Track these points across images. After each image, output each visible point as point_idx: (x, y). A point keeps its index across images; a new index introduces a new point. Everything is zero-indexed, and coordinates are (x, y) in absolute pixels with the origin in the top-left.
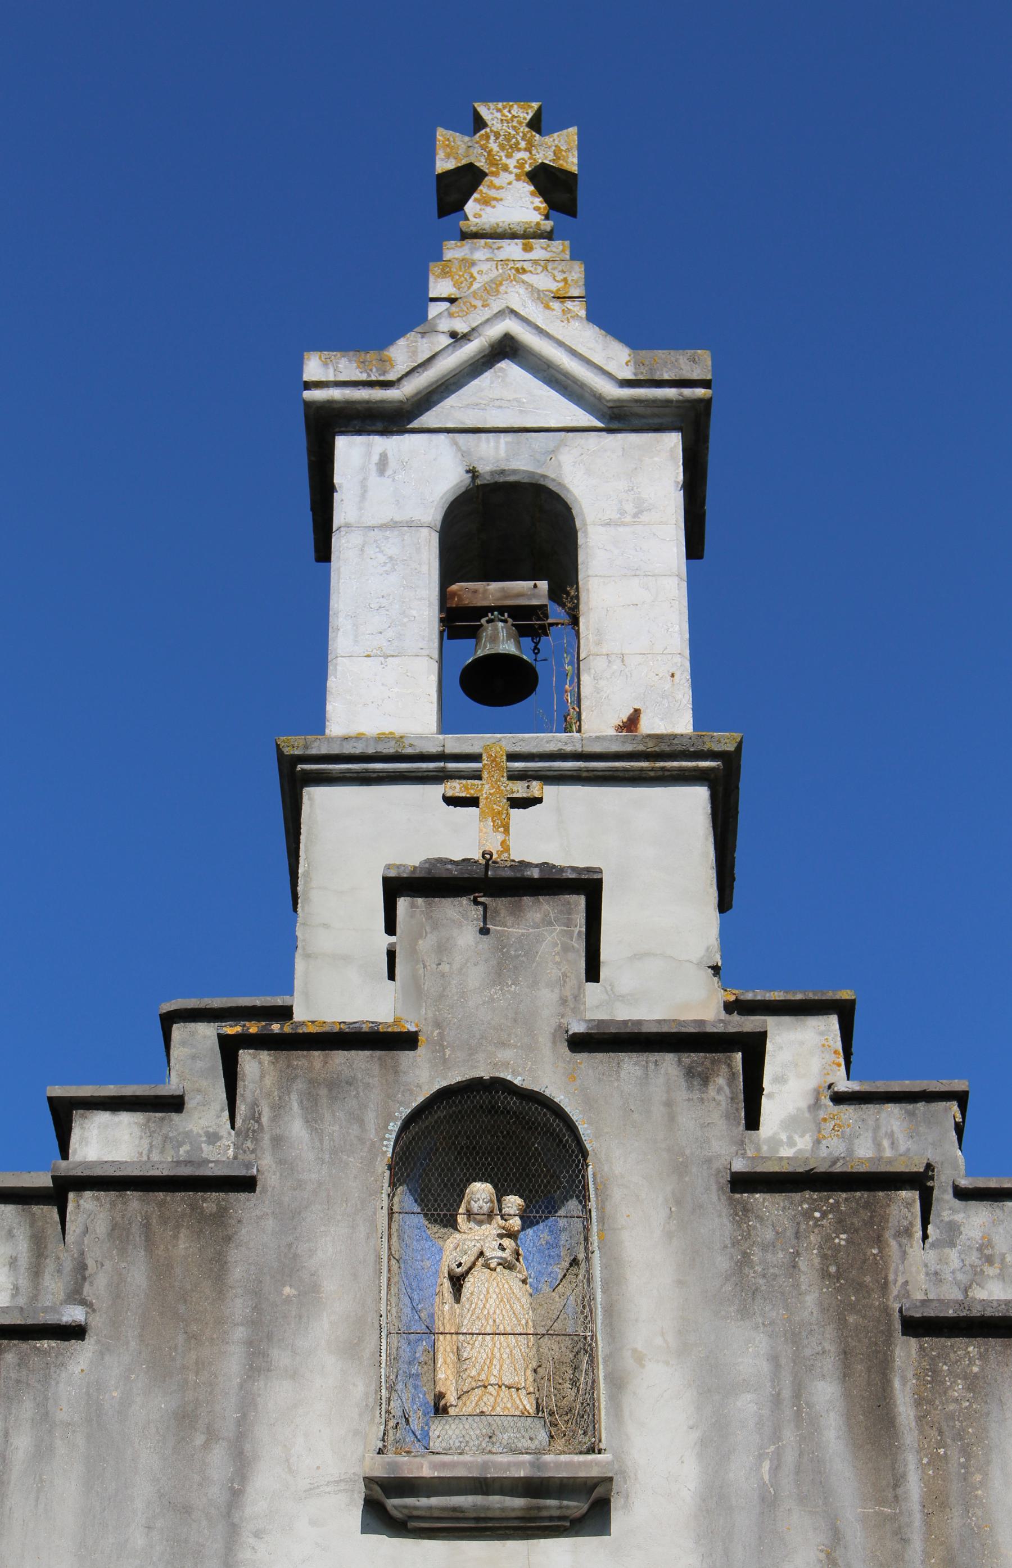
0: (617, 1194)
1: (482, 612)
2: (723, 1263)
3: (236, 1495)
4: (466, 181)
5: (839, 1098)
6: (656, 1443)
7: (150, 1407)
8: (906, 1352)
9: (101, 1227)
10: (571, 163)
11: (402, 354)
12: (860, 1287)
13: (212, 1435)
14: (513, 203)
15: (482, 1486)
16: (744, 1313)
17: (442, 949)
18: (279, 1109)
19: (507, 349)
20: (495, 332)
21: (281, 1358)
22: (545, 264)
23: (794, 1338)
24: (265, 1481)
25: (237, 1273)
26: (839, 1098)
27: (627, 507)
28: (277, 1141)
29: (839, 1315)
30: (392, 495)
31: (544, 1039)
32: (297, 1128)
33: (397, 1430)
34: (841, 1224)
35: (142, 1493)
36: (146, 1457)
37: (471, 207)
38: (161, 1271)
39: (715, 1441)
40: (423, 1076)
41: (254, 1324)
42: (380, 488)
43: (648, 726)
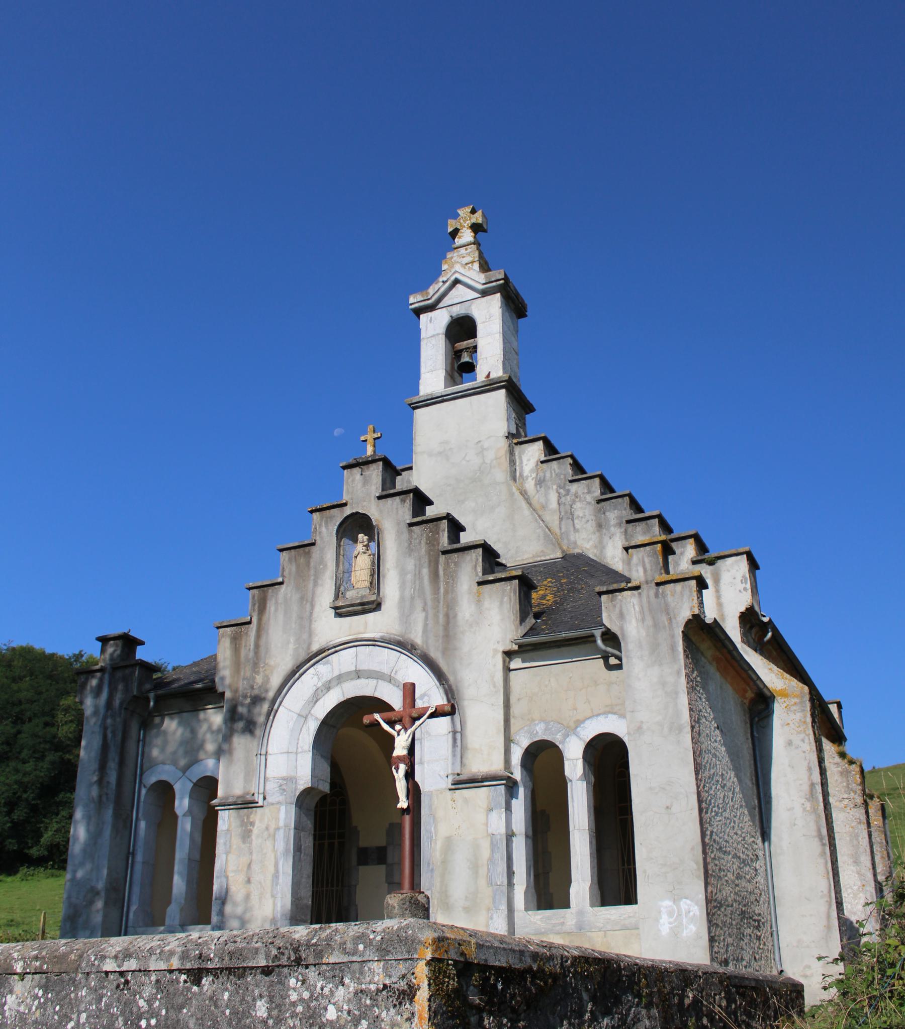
0: (386, 532)
1: (461, 351)
2: (406, 544)
3: (311, 613)
4: (455, 233)
5: (542, 462)
6: (391, 590)
7: (296, 597)
8: (442, 558)
9: (287, 559)
10: (480, 221)
11: (431, 291)
12: (433, 545)
13: (307, 601)
14: (467, 236)
15: (352, 605)
16: (410, 555)
17: (353, 481)
18: (320, 525)
19: (457, 282)
20: (453, 278)
21: (320, 582)
22: (468, 254)
23: (420, 559)
24: (317, 609)
25: (312, 564)
26: (542, 462)
27: (489, 316)
28: (320, 533)
29: (429, 553)
30: (433, 327)
31: (373, 498)
32: (324, 529)
33: (337, 597)
34: (431, 531)
35: (294, 616)
36: (295, 608)
37: (456, 240)
38: (298, 566)
39: (403, 586)
40: (348, 511)
41: (315, 575)
42: (430, 326)
43: (492, 376)
